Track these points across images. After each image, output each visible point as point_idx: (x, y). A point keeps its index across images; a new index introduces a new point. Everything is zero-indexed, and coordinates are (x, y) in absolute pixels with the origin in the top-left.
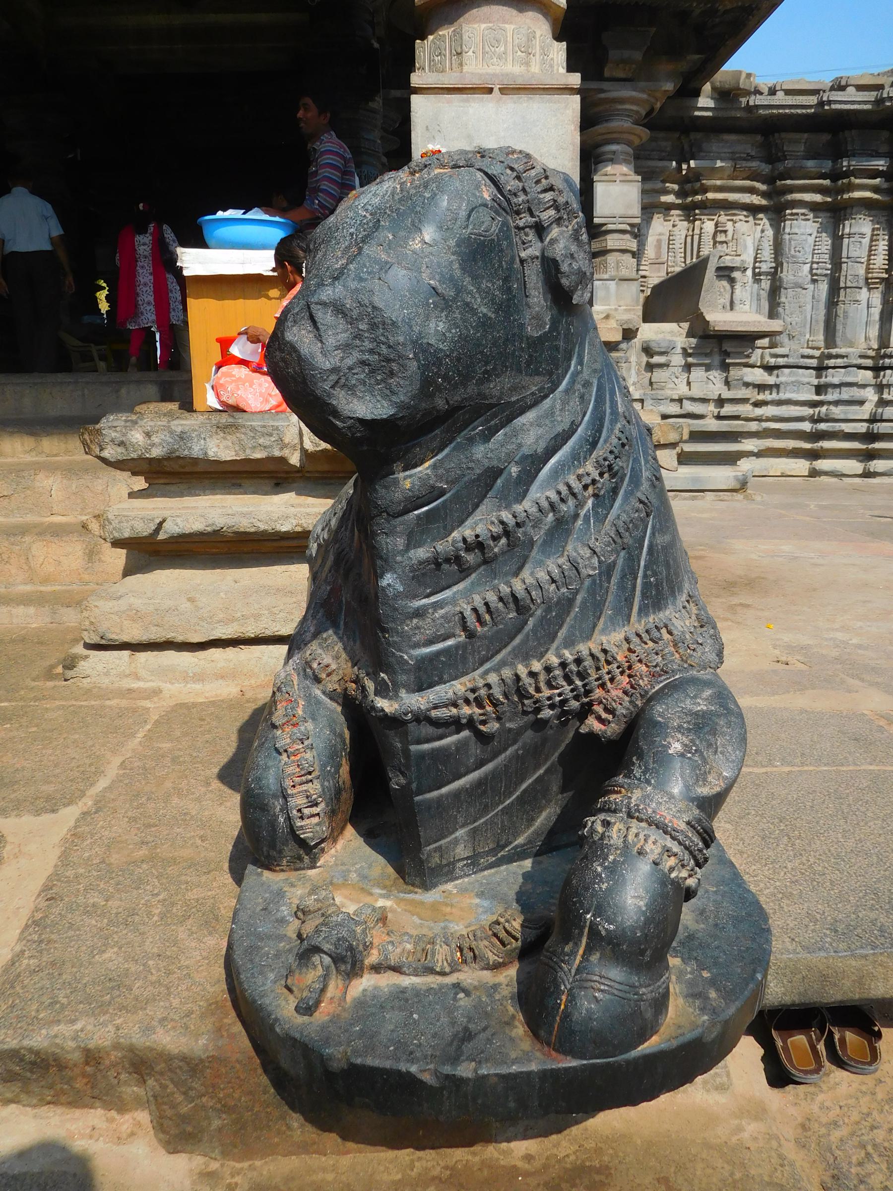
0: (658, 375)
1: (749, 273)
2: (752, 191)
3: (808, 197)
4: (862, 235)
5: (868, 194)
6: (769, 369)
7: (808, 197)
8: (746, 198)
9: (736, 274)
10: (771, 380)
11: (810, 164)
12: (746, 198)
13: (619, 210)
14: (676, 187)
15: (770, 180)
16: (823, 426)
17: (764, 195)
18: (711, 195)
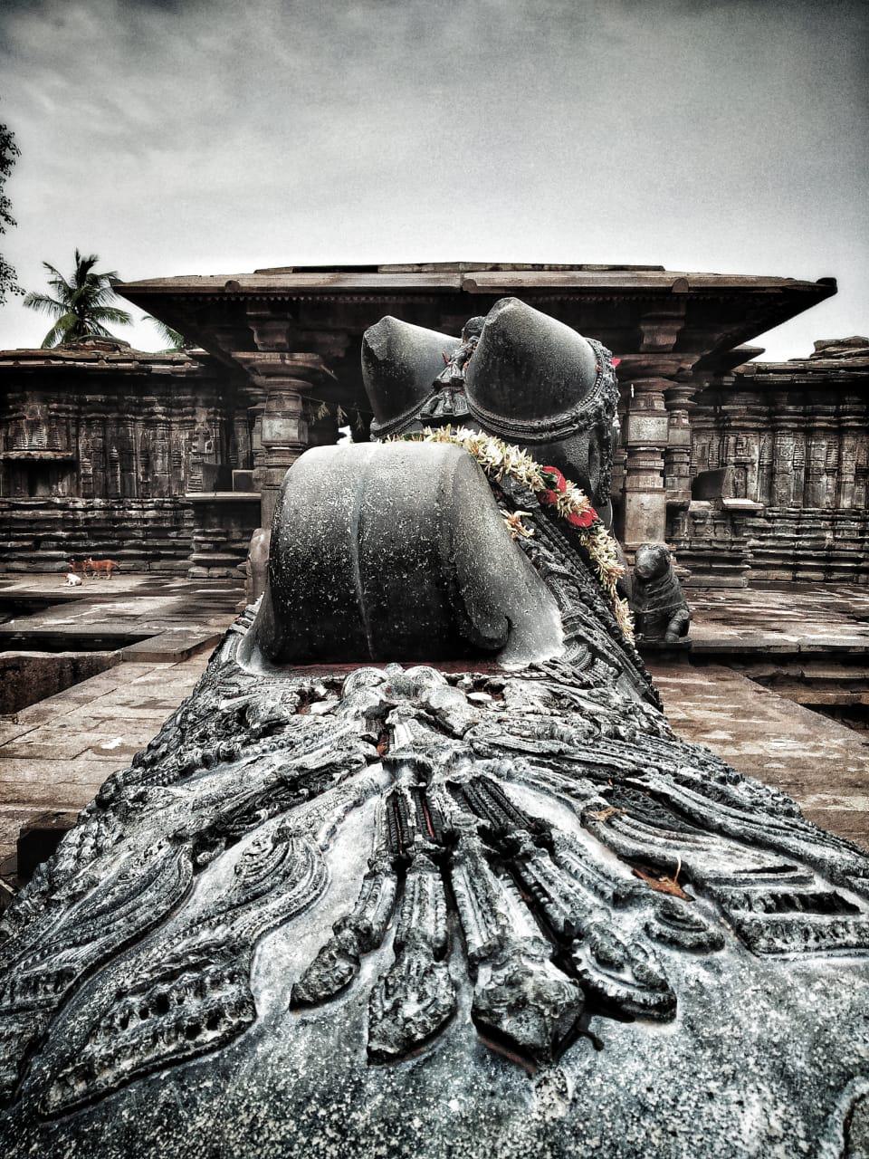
0: (699, 530)
1: (756, 465)
2: (757, 421)
3: (790, 425)
4: (823, 446)
5: (824, 424)
6: (769, 519)
7: (790, 425)
8: (754, 425)
9: (749, 467)
10: (769, 525)
11: (791, 408)
12: (754, 425)
13: (681, 442)
14: (713, 419)
15: (769, 414)
16: (800, 552)
17: (764, 422)
18: (733, 424)
